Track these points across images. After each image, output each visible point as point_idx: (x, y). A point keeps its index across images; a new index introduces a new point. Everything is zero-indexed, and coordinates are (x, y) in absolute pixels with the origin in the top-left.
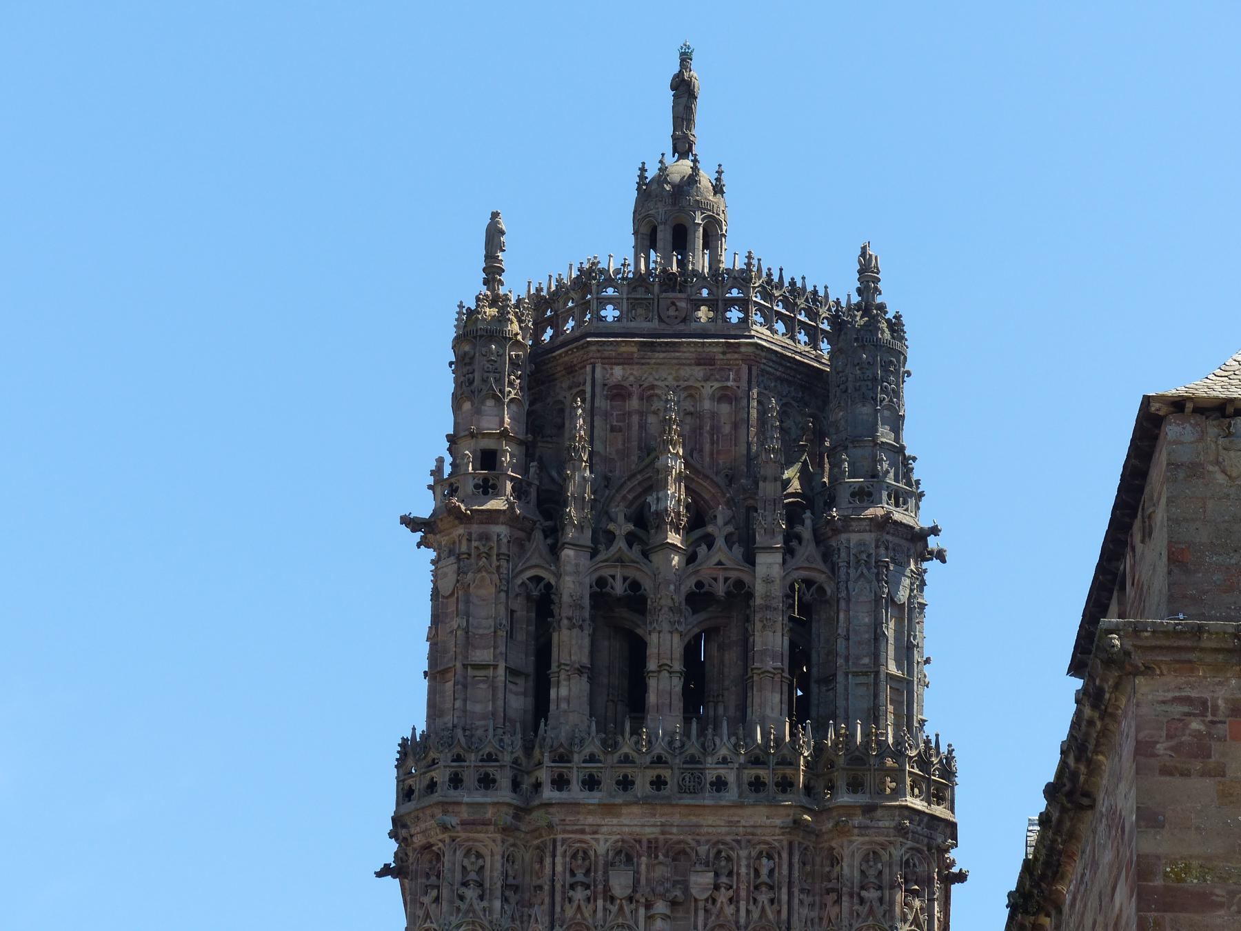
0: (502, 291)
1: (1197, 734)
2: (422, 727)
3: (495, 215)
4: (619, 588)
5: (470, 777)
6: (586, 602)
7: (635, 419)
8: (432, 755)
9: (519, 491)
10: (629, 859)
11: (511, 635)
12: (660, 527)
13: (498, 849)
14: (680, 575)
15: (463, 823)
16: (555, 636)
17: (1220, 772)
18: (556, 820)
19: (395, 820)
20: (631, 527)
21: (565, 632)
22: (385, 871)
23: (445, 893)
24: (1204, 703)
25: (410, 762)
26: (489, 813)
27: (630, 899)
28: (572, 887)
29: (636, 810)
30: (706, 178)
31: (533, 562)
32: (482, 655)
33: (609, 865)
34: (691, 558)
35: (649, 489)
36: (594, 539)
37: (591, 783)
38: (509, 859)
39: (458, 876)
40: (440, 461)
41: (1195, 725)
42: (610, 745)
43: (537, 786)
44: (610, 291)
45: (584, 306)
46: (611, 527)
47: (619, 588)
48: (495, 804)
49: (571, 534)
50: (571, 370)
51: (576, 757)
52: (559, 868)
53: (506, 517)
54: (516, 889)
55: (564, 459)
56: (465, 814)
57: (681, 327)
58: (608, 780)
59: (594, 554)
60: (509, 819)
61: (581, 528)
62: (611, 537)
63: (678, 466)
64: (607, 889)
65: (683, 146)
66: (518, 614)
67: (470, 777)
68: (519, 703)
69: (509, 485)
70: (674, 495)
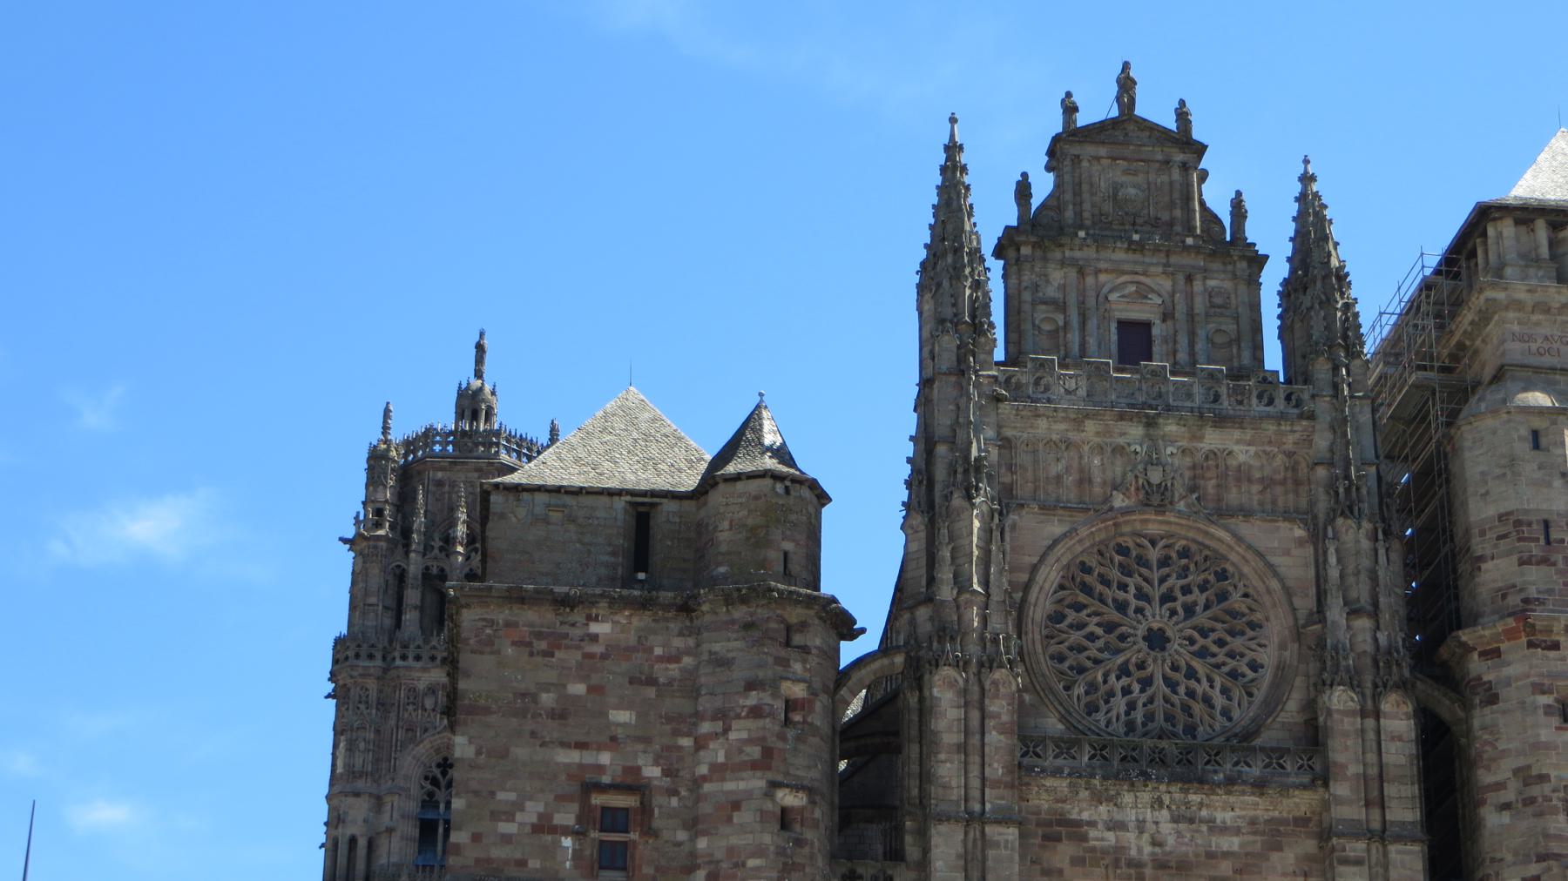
0: (389, 437)
1: (489, 636)
2: (345, 631)
3: (388, 403)
4: (435, 571)
5: (363, 654)
6: (420, 576)
7: (447, 496)
8: (348, 644)
9: (391, 527)
10: (434, 692)
11: (386, 591)
12: (454, 545)
13: (375, 687)
14: (463, 566)
15: (360, 675)
16: (405, 592)
17: (498, 652)
18: (401, 674)
19: (331, 673)
20: (441, 544)
21: (409, 590)
22: (329, 696)
23: (351, 707)
24: (493, 621)
25: (339, 647)
26: (372, 671)
27: (434, 710)
28: (408, 704)
29: (437, 670)
30: (488, 388)
31: (399, 558)
32: (373, 600)
33: (425, 694)
34: (468, 558)
35: (450, 528)
36: (425, 549)
37: (418, 658)
38: (380, 691)
39: (357, 698)
40: (358, 513)
41: (488, 631)
42: (426, 641)
43: (394, 659)
44: (438, 438)
45: (426, 445)
46: (433, 543)
47: (435, 571)
48: (374, 667)
49: (414, 547)
50: (419, 473)
51: (411, 646)
52: (402, 696)
53: (385, 538)
54: (383, 705)
55: (414, 512)
56: (361, 671)
57: (469, 455)
58: (425, 656)
59: (424, 555)
60: (380, 673)
61: (419, 544)
62: (433, 547)
63: (463, 517)
64: (423, 705)
65: (479, 374)
66: (390, 582)
67: (363, 654)
68: (388, 622)
69: (387, 524)
70: (461, 530)
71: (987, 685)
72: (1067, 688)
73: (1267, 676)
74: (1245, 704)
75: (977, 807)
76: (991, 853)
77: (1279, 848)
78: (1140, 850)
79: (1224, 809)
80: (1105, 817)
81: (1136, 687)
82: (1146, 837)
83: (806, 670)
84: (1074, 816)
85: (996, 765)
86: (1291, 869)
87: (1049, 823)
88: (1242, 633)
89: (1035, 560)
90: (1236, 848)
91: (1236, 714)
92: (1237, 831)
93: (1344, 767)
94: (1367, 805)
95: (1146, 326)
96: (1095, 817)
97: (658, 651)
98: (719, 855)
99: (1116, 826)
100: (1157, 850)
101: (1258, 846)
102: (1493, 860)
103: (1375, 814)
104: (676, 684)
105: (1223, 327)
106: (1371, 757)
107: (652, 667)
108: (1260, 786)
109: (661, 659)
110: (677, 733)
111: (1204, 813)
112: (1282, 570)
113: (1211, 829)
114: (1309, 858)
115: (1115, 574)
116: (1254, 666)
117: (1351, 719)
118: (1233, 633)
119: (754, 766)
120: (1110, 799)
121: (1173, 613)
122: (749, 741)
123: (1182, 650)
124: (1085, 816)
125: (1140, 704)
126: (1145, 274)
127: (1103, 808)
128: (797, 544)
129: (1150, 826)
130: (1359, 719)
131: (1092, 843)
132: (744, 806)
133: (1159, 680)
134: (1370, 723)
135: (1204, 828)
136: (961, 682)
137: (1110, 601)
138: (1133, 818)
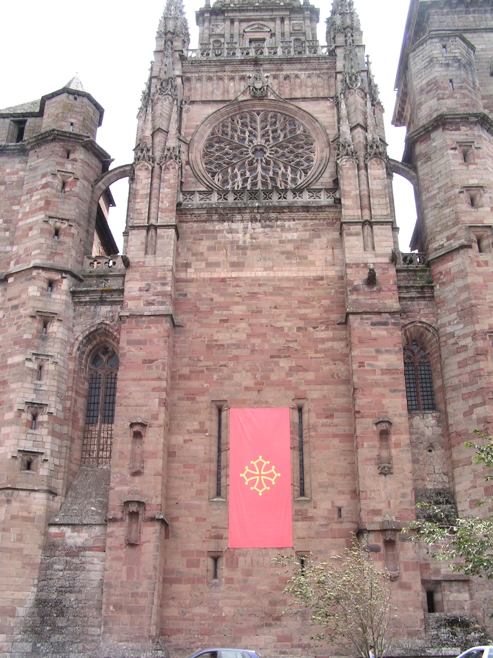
71: (163, 167)
72: (213, 176)
74: (303, 177)
75: (153, 221)
76: (159, 241)
77: (319, 237)
78: (244, 242)
79: (289, 220)
80: (227, 228)
81: (248, 174)
82: (248, 235)
83: (73, 169)
85: (165, 202)
86: (325, 246)
87: (198, 232)
88: (302, 148)
89: (198, 123)
91: (299, 182)
92: (297, 230)
93: (350, 192)
94: (362, 208)
95: (264, 40)
96: (222, 228)
97: (8, 171)
98: (21, 252)
99: (231, 231)
100: (254, 240)
101: (307, 236)
103: (366, 212)
104: (14, 184)
105: (299, 37)
106: (364, 187)
107: (4, 177)
109: (9, 174)
110: (12, 204)
111: (279, 223)
113: (282, 231)
114: (334, 241)
116: (308, 160)
117: (353, 171)
118: (297, 147)
119: (41, 209)
120: (228, 220)
121: (267, 140)
122: (41, 199)
123: (271, 156)
124: (217, 228)
125: (249, 181)
126: (262, 20)
127: (226, 224)
128: (78, 120)
130: (357, 170)
132: (34, 227)
133: (259, 169)
134: (363, 172)
135: (279, 230)
136: (150, 168)
137: (236, 139)
138: (242, 227)
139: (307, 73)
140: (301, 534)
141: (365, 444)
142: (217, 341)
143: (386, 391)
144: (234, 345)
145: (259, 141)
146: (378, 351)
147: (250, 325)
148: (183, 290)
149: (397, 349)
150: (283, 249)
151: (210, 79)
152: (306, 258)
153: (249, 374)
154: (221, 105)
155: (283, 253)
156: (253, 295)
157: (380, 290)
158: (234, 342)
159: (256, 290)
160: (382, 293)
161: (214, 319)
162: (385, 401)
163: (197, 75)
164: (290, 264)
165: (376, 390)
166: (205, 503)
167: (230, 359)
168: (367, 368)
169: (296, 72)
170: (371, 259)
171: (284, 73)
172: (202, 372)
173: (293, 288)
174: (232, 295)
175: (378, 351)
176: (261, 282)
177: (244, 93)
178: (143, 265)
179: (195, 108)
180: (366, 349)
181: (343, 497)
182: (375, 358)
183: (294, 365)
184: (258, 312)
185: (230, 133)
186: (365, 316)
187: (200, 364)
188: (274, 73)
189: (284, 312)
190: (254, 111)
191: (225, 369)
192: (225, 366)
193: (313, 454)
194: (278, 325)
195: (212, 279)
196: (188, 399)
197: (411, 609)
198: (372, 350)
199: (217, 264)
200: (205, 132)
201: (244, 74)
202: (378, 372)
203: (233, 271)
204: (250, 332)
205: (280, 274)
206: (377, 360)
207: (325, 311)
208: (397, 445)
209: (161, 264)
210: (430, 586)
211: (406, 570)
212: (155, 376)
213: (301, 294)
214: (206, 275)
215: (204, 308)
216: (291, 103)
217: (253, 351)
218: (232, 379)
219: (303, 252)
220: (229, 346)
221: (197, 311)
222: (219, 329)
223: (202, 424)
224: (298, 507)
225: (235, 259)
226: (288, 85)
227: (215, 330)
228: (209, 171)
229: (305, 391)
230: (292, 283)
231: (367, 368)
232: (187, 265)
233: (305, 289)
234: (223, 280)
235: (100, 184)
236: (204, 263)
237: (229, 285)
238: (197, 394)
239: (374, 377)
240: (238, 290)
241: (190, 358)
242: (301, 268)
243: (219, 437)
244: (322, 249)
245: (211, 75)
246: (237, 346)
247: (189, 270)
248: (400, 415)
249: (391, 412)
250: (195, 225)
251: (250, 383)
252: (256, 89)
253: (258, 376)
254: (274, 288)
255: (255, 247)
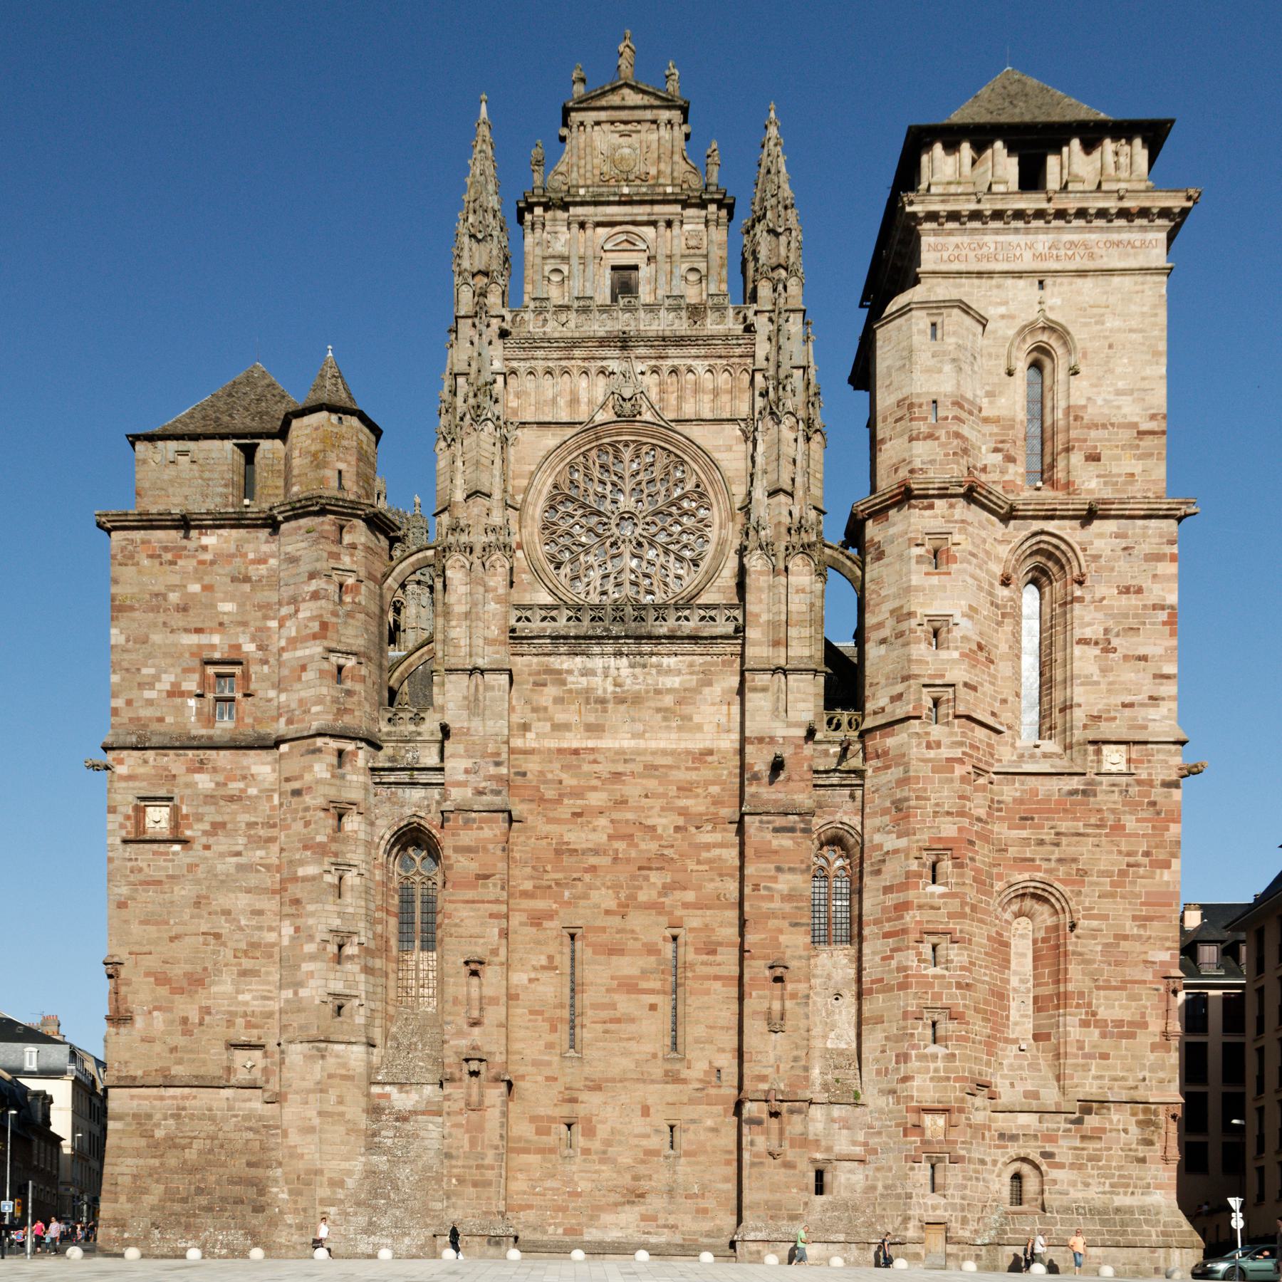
72: (557, 568)
73: (710, 549)
77: (710, 684)
78: (605, 690)
80: (580, 666)
82: (610, 679)
84: (557, 667)
86: (718, 699)
87: (538, 673)
89: (533, 468)
90: (677, 685)
92: (679, 673)
96: (572, 667)
99: (586, 672)
100: (618, 689)
101: (694, 683)
102: (871, 685)
108: (694, 638)
111: (654, 659)
112: (723, 464)
113: (659, 673)
115: (596, 473)
123: (645, 533)
124: (565, 666)
125: (612, 577)
127: (578, 659)
129: (613, 672)
131: (569, 686)
135: (654, 671)
137: (592, 498)
139: (706, 363)
140: (670, 1101)
141: (754, 994)
142: (568, 843)
143: (785, 924)
144: (591, 850)
145: (626, 502)
146: (779, 869)
147: (612, 821)
148: (520, 766)
149: (804, 866)
150: (659, 705)
151: (549, 372)
152: (690, 719)
153: (610, 891)
154: (570, 431)
155: (659, 710)
156: (617, 776)
157: (789, 779)
158: (590, 846)
159: (620, 768)
160: (791, 784)
161: (564, 811)
162: (782, 939)
163: (528, 364)
164: (668, 728)
165: (773, 923)
166: (556, 1059)
167: (586, 870)
168: (763, 892)
169: (689, 362)
170: (780, 731)
171: (670, 362)
172: (550, 887)
173: (670, 767)
174: (588, 775)
175: (779, 869)
176: (627, 757)
177: (603, 406)
178: (468, 732)
179: (524, 435)
180: (763, 866)
181: (723, 1055)
182: (774, 879)
183: (668, 880)
184: (622, 803)
185: (582, 485)
186: (765, 818)
187: (546, 876)
188: (653, 362)
189: (658, 803)
190: (619, 442)
191: (579, 884)
192: (579, 879)
193: (689, 1002)
194: (649, 822)
195: (560, 751)
196: (532, 925)
197: (795, 1190)
198: (772, 866)
199: (566, 727)
200: (544, 483)
201: (604, 363)
202: (777, 897)
203: (589, 738)
204: (611, 831)
205: (653, 745)
206: (776, 882)
207: (714, 803)
208: (794, 996)
209: (493, 731)
210: (821, 1166)
211: (792, 1146)
212: (492, 898)
213: (681, 775)
214: (553, 744)
215: (550, 794)
216: (679, 428)
217: (615, 859)
218: (589, 899)
219: (687, 710)
220: (585, 852)
221: (542, 800)
222: (571, 826)
223: (551, 958)
224: (669, 1067)
225: (591, 719)
226: (675, 388)
227: (566, 827)
228: (552, 558)
229: (681, 918)
230: (670, 758)
231: (763, 892)
232: (525, 727)
233: (687, 769)
234: (576, 752)
235: (390, 580)
236: (549, 724)
237: (584, 759)
238: (545, 918)
239: (772, 905)
240: (596, 767)
241: (533, 867)
242: (684, 735)
243: (573, 974)
244: (713, 704)
245: (551, 364)
246: (596, 852)
247: (530, 735)
248: (800, 957)
249: (789, 953)
250: (535, 659)
251: (612, 905)
252: (624, 400)
253: (622, 895)
254: (646, 767)
255: (622, 701)
